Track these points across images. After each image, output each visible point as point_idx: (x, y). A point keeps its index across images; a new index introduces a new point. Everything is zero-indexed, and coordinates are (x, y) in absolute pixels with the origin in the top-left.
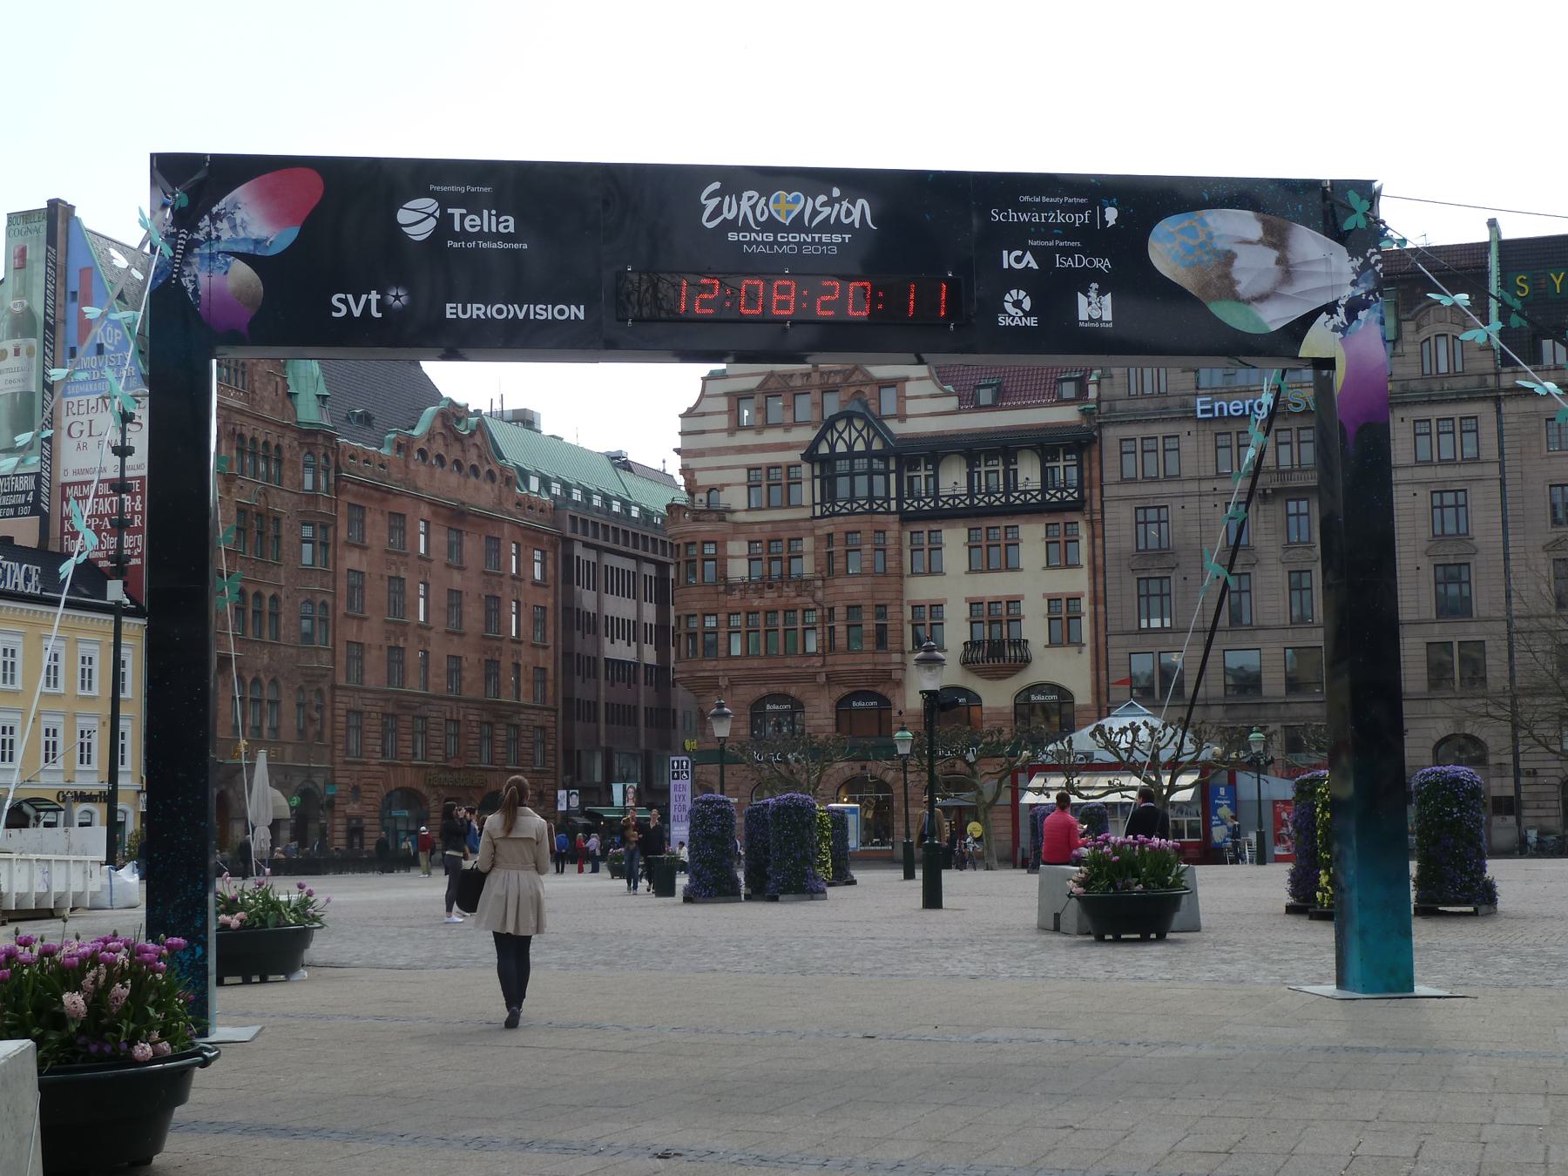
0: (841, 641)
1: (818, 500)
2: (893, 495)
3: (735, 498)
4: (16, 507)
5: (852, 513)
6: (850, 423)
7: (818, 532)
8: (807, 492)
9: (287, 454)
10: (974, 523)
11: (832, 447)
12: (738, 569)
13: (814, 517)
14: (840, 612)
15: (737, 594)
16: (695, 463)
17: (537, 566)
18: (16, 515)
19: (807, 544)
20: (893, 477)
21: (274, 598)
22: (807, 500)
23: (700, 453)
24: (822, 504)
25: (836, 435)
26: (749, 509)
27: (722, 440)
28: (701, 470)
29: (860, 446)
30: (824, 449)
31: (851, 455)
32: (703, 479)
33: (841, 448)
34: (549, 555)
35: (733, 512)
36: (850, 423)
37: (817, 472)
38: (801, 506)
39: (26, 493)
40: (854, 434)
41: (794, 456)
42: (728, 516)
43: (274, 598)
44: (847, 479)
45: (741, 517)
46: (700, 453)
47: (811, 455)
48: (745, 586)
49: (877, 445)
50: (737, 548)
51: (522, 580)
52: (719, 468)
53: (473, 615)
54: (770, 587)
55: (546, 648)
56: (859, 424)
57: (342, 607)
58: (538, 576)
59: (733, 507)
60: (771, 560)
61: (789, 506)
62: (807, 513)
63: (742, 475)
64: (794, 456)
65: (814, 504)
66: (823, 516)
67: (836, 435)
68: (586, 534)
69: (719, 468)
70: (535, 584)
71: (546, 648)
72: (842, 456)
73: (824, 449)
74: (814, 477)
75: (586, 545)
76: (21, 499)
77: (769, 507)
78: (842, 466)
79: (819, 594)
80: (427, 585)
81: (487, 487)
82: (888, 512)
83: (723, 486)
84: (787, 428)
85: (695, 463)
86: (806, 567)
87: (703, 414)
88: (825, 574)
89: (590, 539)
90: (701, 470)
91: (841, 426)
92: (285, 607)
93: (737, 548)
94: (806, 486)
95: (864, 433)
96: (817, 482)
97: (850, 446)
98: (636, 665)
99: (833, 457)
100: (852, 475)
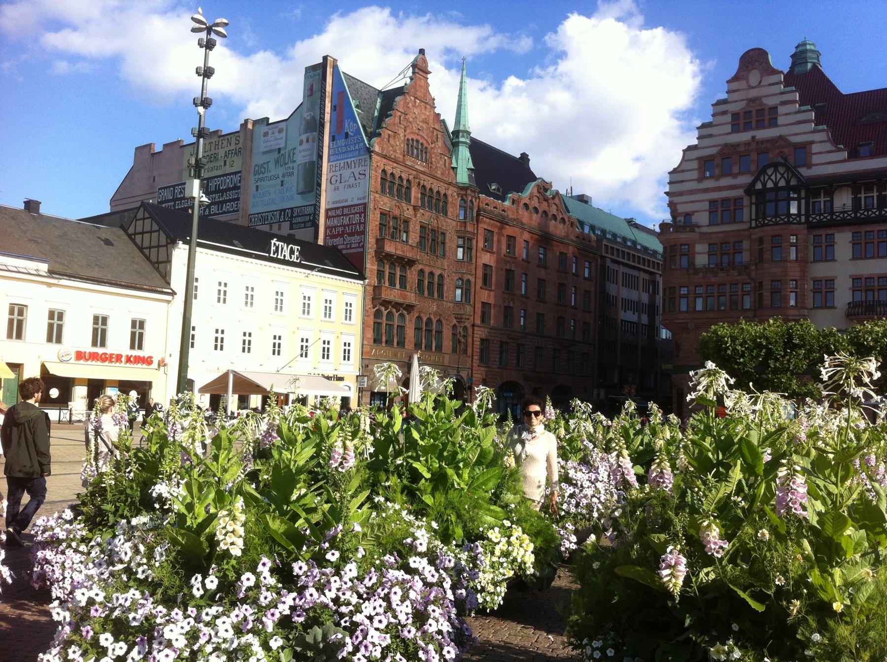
0: (767, 300)
1: (753, 217)
2: (803, 212)
3: (702, 218)
4: (304, 223)
5: (776, 224)
6: (776, 170)
7: (753, 237)
8: (747, 213)
9: (450, 199)
10: (856, 229)
11: (764, 184)
12: (701, 260)
13: (751, 228)
14: (767, 284)
15: (701, 275)
16: (676, 200)
17: (587, 270)
18: (305, 227)
19: (746, 244)
20: (803, 201)
21: (441, 276)
22: (746, 217)
23: (681, 194)
24: (756, 220)
25: (767, 177)
26: (710, 225)
27: (694, 185)
28: (680, 203)
29: (782, 183)
30: (759, 186)
31: (776, 188)
32: (681, 209)
33: (770, 185)
34: (593, 264)
35: (699, 227)
36: (776, 170)
37: (754, 201)
38: (743, 222)
39: (310, 215)
40: (779, 176)
41: (740, 192)
42: (697, 229)
43: (441, 276)
44: (773, 204)
45: (705, 230)
46: (681, 194)
47: (750, 190)
48: (706, 270)
49: (793, 182)
50: (701, 248)
51: (578, 276)
52: (692, 202)
53: (551, 293)
54: (722, 270)
55: (590, 312)
56: (782, 170)
57: (480, 283)
58: (586, 275)
59: (700, 224)
60: (722, 254)
61: (735, 222)
62: (745, 226)
63: (706, 206)
64: (740, 192)
65: (751, 220)
66: (757, 227)
67: (767, 177)
68: (613, 254)
69: (692, 202)
70: (585, 279)
71: (590, 312)
72: (770, 190)
73: (759, 186)
74: (751, 204)
75: (613, 261)
76: (307, 218)
77: (722, 223)
78: (770, 196)
79: (753, 274)
80: (526, 275)
81: (561, 226)
82: (799, 223)
83: (694, 212)
84: (735, 176)
85: (676, 200)
86: (745, 257)
87: (683, 171)
88: (757, 261)
89: (615, 258)
90: (680, 203)
91: (770, 171)
92: (447, 281)
93: (701, 248)
94: (746, 211)
95: (785, 175)
96: (754, 207)
97: (776, 184)
98: (637, 324)
99: (765, 190)
100: (776, 201)
